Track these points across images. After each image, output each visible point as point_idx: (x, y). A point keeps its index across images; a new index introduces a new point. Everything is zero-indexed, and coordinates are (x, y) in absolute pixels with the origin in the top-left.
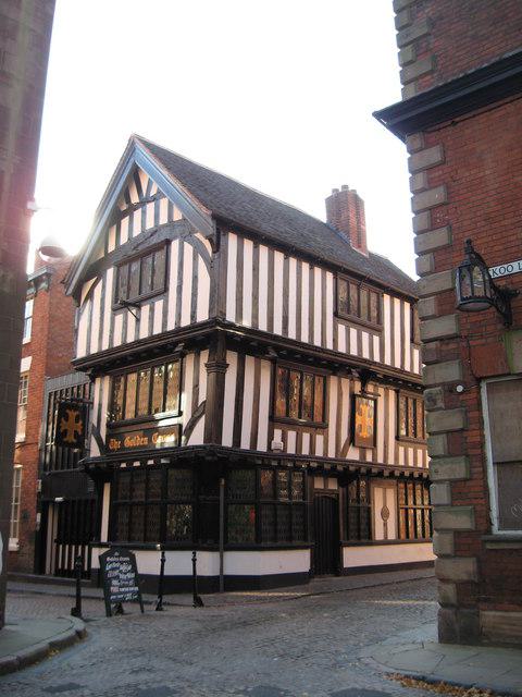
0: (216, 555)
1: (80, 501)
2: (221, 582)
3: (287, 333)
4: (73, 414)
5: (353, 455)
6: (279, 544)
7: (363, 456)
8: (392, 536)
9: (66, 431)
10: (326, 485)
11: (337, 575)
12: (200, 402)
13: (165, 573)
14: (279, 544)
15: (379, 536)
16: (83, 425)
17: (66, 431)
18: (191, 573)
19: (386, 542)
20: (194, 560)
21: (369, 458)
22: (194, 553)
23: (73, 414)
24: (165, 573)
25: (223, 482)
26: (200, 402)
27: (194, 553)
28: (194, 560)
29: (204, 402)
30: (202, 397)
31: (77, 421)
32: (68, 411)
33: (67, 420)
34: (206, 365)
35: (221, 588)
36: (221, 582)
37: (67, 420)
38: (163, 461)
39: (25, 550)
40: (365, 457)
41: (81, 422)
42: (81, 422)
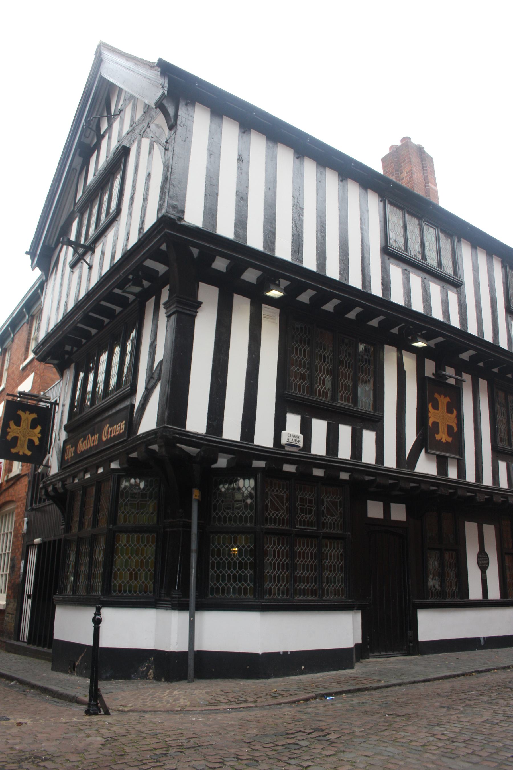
1: (55, 541)
2: (191, 662)
3: (301, 261)
6: (298, 599)
7: (442, 468)
8: (494, 593)
10: (387, 511)
11: (409, 653)
13: (104, 643)
14: (298, 599)
21: (453, 473)
22: (98, 612)
23: (27, 417)
24: (104, 643)
25: (196, 494)
29: (161, 363)
30: (159, 356)
32: (20, 413)
33: (18, 423)
36: (191, 662)
37: (18, 423)
38: (114, 465)
39: (11, 606)
40: (446, 474)
41: (39, 428)
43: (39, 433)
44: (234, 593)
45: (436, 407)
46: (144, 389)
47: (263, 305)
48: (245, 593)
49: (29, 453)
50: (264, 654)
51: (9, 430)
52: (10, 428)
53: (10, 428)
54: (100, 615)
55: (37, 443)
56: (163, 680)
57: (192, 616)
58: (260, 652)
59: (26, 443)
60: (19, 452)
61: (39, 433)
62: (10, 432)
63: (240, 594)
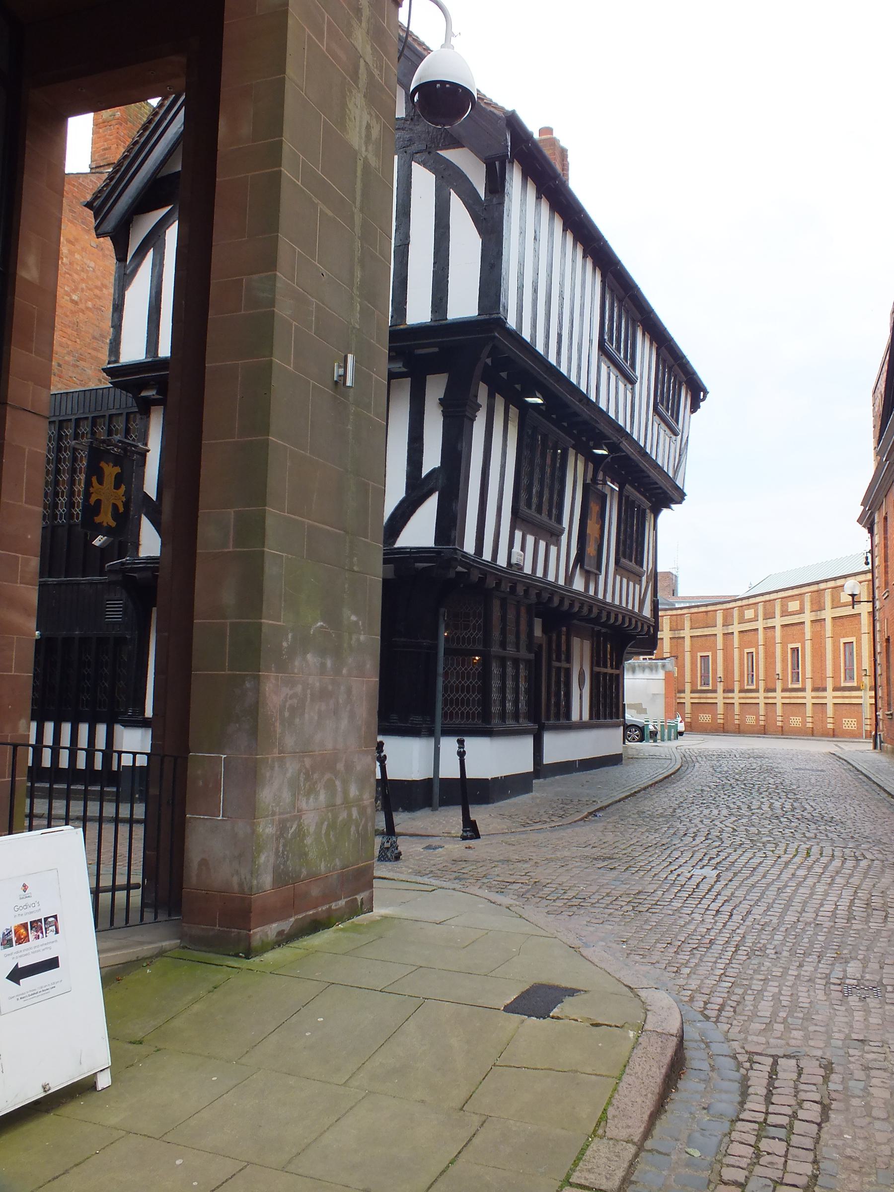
0: (431, 742)
4: (110, 471)
5: (578, 584)
8: (586, 717)
9: (99, 502)
12: (425, 472)
15: (575, 717)
16: (127, 493)
17: (99, 502)
18: (457, 775)
19: (582, 726)
20: (462, 754)
26: (425, 471)
27: (461, 743)
28: (462, 754)
30: (432, 460)
31: (117, 487)
34: (442, 402)
35: (436, 799)
42: (123, 487)
43: (123, 496)
44: (462, 718)
45: (591, 520)
46: (402, 495)
47: (511, 406)
48: (473, 719)
49: (113, 524)
50: (492, 778)
51: (91, 490)
52: (93, 487)
53: (93, 487)
54: (463, 748)
55: (121, 509)
56: (400, 809)
57: (437, 744)
58: (489, 777)
59: (110, 509)
60: (103, 522)
61: (123, 496)
62: (92, 493)
63: (468, 718)
